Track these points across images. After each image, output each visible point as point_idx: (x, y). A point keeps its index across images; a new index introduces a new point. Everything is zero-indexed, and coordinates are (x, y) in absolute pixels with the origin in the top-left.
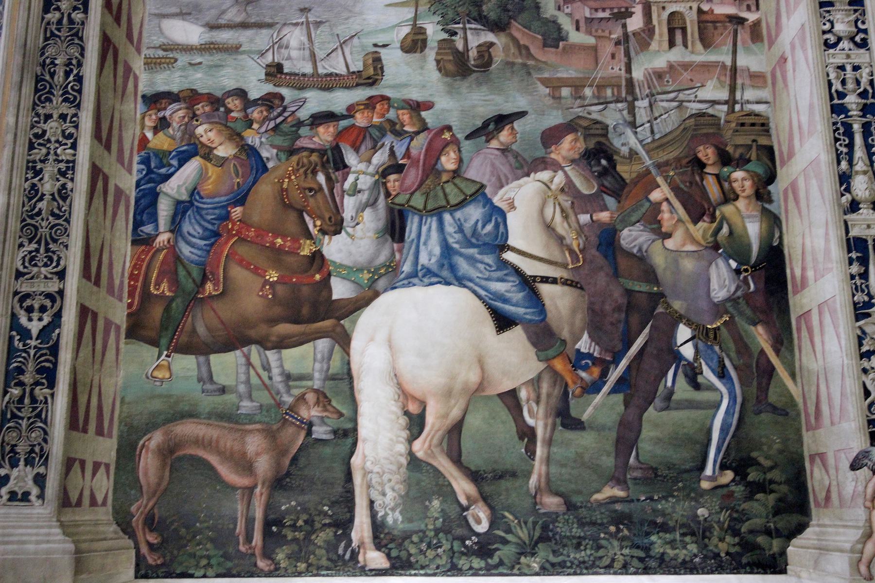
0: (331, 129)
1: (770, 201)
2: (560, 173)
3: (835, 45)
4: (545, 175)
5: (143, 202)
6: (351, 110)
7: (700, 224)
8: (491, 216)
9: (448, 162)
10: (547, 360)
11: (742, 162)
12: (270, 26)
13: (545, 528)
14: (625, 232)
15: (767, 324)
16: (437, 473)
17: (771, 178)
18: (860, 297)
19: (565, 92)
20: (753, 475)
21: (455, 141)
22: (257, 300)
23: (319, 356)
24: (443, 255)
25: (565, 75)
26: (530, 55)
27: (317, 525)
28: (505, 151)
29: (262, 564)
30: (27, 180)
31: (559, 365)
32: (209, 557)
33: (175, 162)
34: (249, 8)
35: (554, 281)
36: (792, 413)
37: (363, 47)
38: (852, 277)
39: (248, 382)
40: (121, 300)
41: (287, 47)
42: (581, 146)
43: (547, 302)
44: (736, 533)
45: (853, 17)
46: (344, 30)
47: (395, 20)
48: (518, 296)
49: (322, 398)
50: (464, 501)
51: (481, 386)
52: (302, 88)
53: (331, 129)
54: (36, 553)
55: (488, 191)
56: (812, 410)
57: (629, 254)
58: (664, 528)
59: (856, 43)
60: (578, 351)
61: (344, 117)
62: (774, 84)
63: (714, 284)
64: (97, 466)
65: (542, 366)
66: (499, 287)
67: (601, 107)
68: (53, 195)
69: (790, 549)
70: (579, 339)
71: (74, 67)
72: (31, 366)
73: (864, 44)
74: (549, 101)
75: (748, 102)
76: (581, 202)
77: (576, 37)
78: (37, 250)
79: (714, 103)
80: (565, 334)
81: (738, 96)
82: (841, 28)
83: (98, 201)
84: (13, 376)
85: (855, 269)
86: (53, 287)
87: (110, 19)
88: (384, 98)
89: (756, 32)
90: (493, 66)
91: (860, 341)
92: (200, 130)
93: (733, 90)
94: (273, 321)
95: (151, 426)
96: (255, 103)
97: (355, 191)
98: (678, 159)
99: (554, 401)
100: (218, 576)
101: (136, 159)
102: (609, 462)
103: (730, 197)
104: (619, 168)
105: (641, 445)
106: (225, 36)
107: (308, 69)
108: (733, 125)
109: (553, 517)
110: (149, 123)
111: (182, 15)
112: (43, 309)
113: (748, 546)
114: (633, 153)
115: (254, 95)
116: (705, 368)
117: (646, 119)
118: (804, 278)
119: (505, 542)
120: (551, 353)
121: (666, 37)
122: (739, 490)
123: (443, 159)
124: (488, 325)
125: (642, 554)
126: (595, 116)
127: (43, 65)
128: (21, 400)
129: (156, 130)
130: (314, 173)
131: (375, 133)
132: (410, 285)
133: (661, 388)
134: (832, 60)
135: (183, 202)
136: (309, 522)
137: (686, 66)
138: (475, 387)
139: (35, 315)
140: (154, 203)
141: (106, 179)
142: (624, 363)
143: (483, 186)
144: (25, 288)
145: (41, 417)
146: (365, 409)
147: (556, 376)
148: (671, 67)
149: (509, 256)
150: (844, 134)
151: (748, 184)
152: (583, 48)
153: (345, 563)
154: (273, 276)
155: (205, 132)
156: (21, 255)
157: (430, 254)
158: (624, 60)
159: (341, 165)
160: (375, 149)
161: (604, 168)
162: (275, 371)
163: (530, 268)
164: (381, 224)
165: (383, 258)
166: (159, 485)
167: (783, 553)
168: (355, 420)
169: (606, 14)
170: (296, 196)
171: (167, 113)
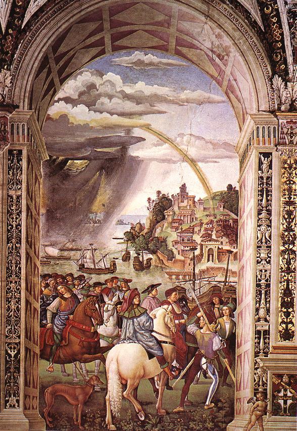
0: (100, 289)
1: (234, 317)
2: (170, 306)
4: (166, 306)
5: (43, 313)
6: (106, 281)
8: (149, 320)
9: (136, 301)
10: (163, 369)
11: (225, 304)
12: (80, 250)
13: (160, 418)
14: (189, 327)
17: (235, 309)
19: (174, 277)
20: (220, 404)
21: (139, 294)
22: (78, 347)
23: (96, 365)
24: (133, 332)
25: (174, 271)
27: (96, 417)
28: (154, 298)
30: (6, 304)
31: (166, 370)
32: (66, 426)
33: (51, 299)
34: (73, 243)
35: (166, 343)
37: (110, 259)
38: (255, 343)
41: (86, 258)
42: (178, 296)
44: (213, 422)
45: (267, 252)
46: (104, 252)
48: (155, 347)
51: (144, 376)
52: (90, 274)
53: (100, 289)
54: (18, 422)
57: (189, 334)
59: (267, 262)
60: (172, 365)
61: (104, 284)
62: (239, 276)
63: (214, 345)
64: (33, 397)
66: (151, 344)
67: (184, 283)
68: (15, 310)
71: (18, 264)
73: (269, 262)
74: (168, 280)
75: (230, 282)
77: (179, 257)
78: (11, 329)
81: (227, 280)
82: (262, 255)
84: (7, 370)
87: (28, 247)
88: (116, 278)
91: (255, 364)
92: (59, 288)
96: (76, 279)
101: (39, 297)
103: (222, 315)
105: (189, 395)
106: (66, 253)
107: (93, 267)
108: (225, 290)
111: (52, 245)
112: (15, 348)
115: (75, 276)
116: (209, 371)
117: (198, 288)
119: (148, 423)
120: (164, 366)
121: (207, 258)
122: (215, 409)
123: (134, 300)
125: (186, 428)
126: (182, 286)
127: (8, 263)
129: (45, 288)
130: (95, 305)
134: (258, 268)
135: (55, 313)
136: (93, 416)
137: (212, 268)
138: (142, 376)
140: (46, 314)
141: (31, 304)
143: (147, 310)
144: (9, 341)
146: (110, 381)
148: (208, 269)
149: (153, 334)
150: (259, 294)
151: (227, 311)
152: (180, 261)
156: (7, 330)
157: (130, 333)
158: (193, 266)
159: (103, 302)
161: (184, 304)
164: (115, 322)
165: (115, 334)
166: (51, 403)
167: (226, 428)
169: (188, 249)
170: (89, 313)
171: (49, 281)
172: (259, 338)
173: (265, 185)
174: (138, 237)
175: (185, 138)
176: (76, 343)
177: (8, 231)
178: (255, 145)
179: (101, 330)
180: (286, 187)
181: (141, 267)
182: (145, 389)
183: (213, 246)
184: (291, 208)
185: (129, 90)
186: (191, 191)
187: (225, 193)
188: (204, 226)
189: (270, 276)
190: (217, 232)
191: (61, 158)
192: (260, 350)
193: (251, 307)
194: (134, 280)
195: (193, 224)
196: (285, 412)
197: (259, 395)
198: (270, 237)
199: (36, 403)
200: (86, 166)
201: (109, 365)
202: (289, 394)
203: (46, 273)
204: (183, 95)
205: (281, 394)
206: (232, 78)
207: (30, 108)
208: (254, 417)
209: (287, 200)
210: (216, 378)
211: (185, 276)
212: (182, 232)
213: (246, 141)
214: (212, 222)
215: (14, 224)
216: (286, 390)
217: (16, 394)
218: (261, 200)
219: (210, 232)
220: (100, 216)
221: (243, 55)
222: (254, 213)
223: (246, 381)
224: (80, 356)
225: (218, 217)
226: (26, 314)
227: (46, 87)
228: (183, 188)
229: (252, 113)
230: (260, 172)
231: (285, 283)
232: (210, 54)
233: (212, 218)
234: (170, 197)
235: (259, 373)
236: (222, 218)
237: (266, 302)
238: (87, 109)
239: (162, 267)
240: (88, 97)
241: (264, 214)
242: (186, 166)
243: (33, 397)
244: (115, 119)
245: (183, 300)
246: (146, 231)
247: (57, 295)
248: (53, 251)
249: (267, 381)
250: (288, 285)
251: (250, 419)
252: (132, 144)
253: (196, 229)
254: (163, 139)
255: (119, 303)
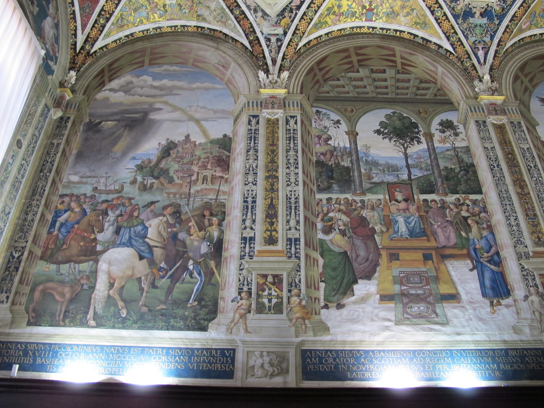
1: (222, 226)
3: (247, 185)
4: (161, 218)
7: (201, 232)
9: (136, 214)
10: (151, 269)
11: (216, 215)
15: (215, 261)
16: (115, 299)
17: (223, 220)
18: (243, 253)
19: (171, 196)
20: (203, 303)
21: (139, 209)
26: (164, 185)
28: (151, 211)
29: (61, 323)
31: (155, 271)
35: (157, 247)
36: (217, 286)
39: (69, 272)
40: (40, 248)
42: (173, 210)
43: (155, 253)
44: (195, 319)
46: (115, 179)
47: (129, 176)
48: (147, 251)
49: (88, 278)
50: (120, 308)
51: (131, 276)
52: (101, 194)
55: (145, 222)
56: (223, 284)
57: (180, 240)
58: (175, 318)
61: (110, 201)
63: (202, 249)
65: (150, 270)
66: (143, 248)
69: (210, 324)
70: (161, 263)
72: (13, 266)
73: (255, 184)
74: (166, 198)
76: (170, 225)
77: (177, 181)
79: (211, 199)
80: (158, 262)
83: (41, 223)
85: (243, 245)
86: (24, 245)
87: (56, 175)
89: (226, 181)
90: (154, 188)
93: (217, 196)
94: (79, 256)
95: (41, 283)
96: (88, 197)
97: (109, 221)
98: (199, 214)
99: (151, 281)
100: (49, 326)
102: (163, 298)
103: (211, 225)
104: (182, 217)
107: (104, 189)
109: (144, 313)
110: (59, 202)
111: (75, 174)
112: (20, 251)
113: (198, 323)
114: (186, 212)
115: (88, 195)
118: (227, 247)
119: (129, 320)
120: (153, 267)
122: (198, 307)
124: (138, 258)
125: (167, 324)
128: (8, 276)
130: (99, 216)
131: (118, 206)
132: (118, 247)
133: (182, 278)
137: (205, 189)
139: (17, 252)
142: (173, 270)
144: (17, 244)
145: (12, 280)
146: (99, 280)
147: (153, 274)
148: (202, 189)
149: (147, 240)
151: (217, 221)
153: (84, 324)
154: (82, 244)
155: (73, 204)
157: (125, 239)
158: (188, 187)
159: (107, 214)
160: (117, 210)
162: (77, 270)
163: (152, 243)
164: (114, 230)
165: (112, 240)
167: (207, 326)
168: (95, 284)
171: (64, 200)
172: (245, 244)
173: (253, 135)
174: (145, 168)
175: (193, 108)
176: (75, 247)
177: (43, 165)
178: (246, 111)
179: (100, 237)
180: (270, 135)
181: (144, 188)
182: (132, 288)
183: (208, 173)
184: (274, 148)
185: (156, 84)
186: (193, 139)
187: (221, 139)
188: (202, 160)
189: (256, 195)
190: (212, 164)
191: (98, 121)
192: (245, 253)
193: (239, 218)
194: (137, 198)
195: (191, 159)
196: (269, 310)
197: (243, 295)
198: (257, 167)
199: (24, 300)
200: (115, 125)
201: (101, 266)
202: (274, 293)
203: (65, 193)
204: (194, 86)
205: (266, 293)
206: (231, 77)
207: (84, 94)
208: (237, 316)
209: (271, 143)
210: (201, 280)
211: (181, 195)
212: (183, 164)
213: (239, 109)
214: (208, 157)
215: (49, 161)
216: (270, 289)
217: (9, 291)
218: (250, 143)
219: (206, 164)
220: (118, 155)
221: (239, 65)
222: (244, 151)
223: (231, 281)
224: (76, 258)
225: (214, 155)
226: (38, 223)
227: (98, 84)
228: (188, 137)
229: (244, 93)
230: (249, 126)
231: (270, 200)
232: (217, 65)
233: (209, 155)
234: (176, 142)
235: (244, 274)
236: (217, 154)
237: (252, 214)
238: (124, 94)
239: (161, 189)
240: (127, 89)
241: (251, 152)
242: (192, 124)
243: (23, 294)
244: (144, 99)
245: (177, 213)
246: (153, 164)
247: (69, 209)
248: (75, 178)
249: (252, 281)
250: (272, 201)
251: (234, 316)
252: (152, 112)
253: (195, 162)
254: (175, 108)
255: (121, 215)
